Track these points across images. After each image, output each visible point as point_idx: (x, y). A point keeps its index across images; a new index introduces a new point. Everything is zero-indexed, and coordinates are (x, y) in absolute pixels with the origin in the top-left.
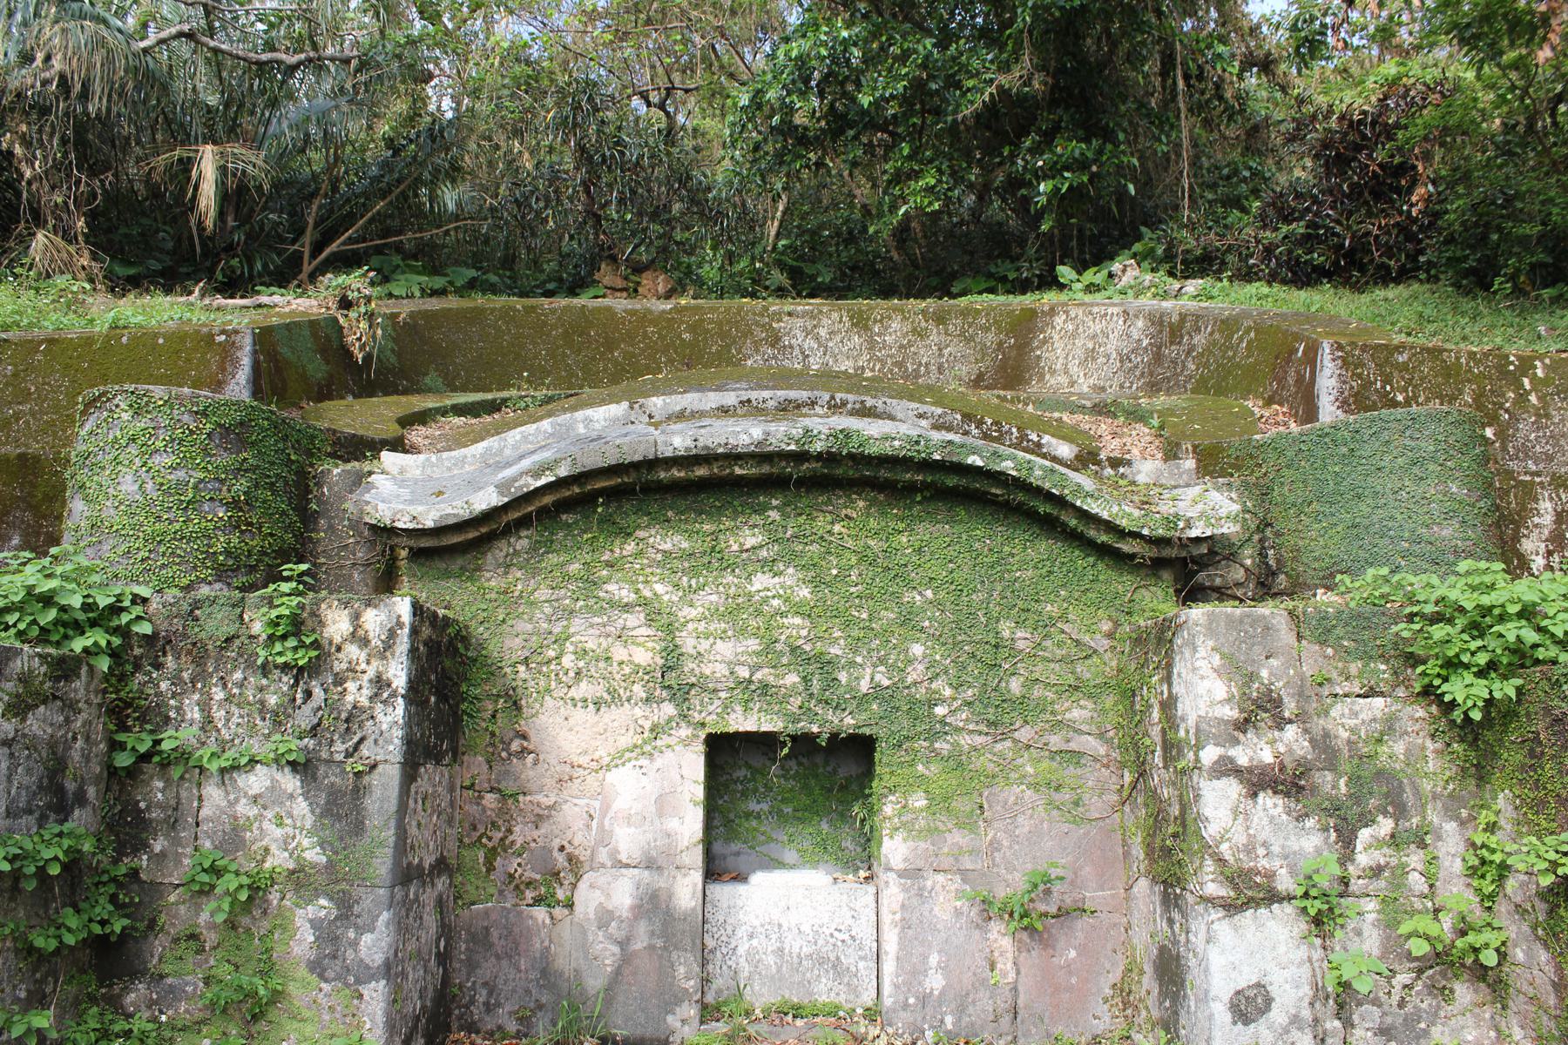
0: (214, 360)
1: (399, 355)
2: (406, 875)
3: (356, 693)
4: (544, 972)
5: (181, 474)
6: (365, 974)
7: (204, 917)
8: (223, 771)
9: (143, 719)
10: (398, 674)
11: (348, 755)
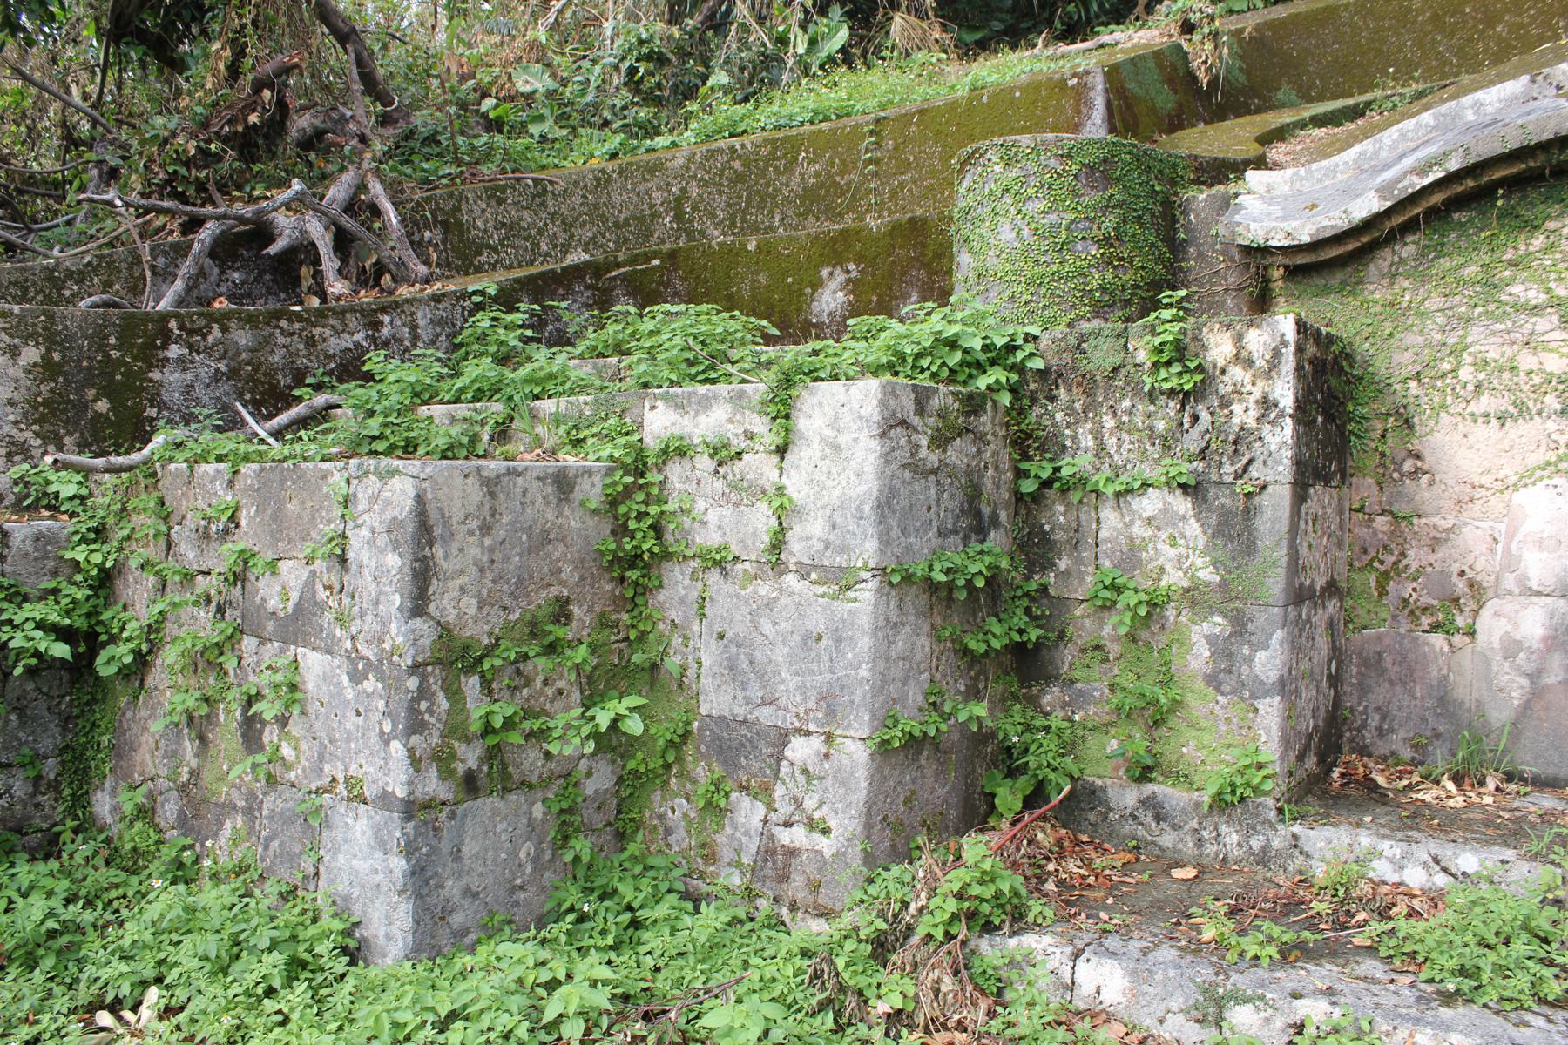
0: (1068, 104)
1: (1248, 73)
2: (1299, 596)
3: (1243, 415)
4: (1443, 700)
5: (1053, 217)
6: (1260, 690)
7: (1107, 630)
8: (1118, 495)
9: (1042, 449)
10: (1285, 393)
11: (1238, 476)
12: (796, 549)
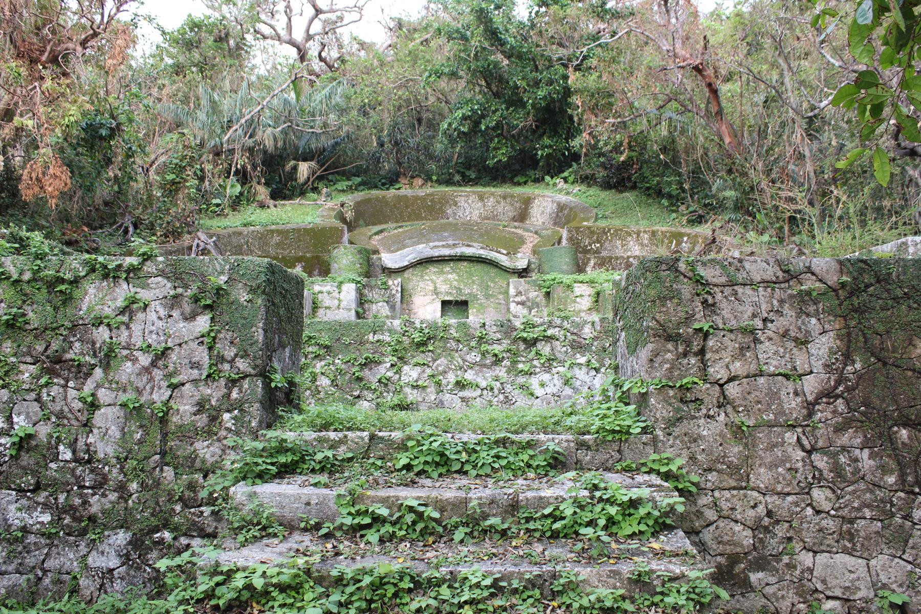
3: (394, 292)
10: (399, 289)
12: (342, 306)
